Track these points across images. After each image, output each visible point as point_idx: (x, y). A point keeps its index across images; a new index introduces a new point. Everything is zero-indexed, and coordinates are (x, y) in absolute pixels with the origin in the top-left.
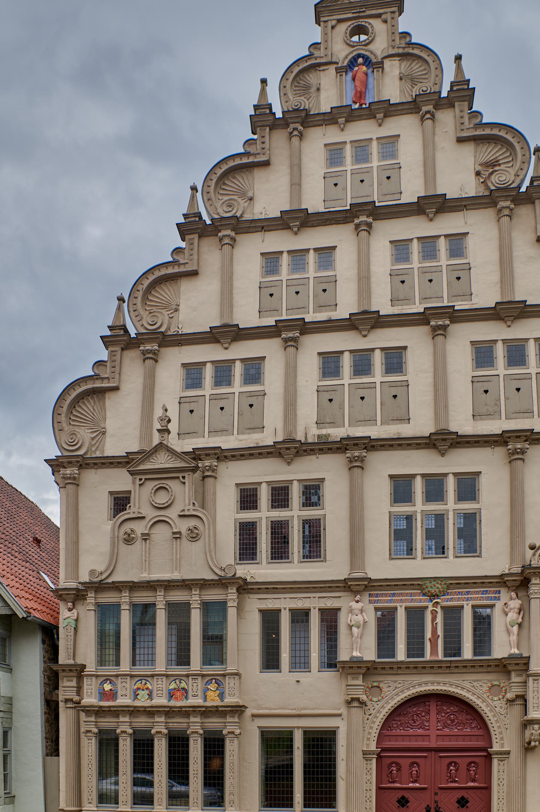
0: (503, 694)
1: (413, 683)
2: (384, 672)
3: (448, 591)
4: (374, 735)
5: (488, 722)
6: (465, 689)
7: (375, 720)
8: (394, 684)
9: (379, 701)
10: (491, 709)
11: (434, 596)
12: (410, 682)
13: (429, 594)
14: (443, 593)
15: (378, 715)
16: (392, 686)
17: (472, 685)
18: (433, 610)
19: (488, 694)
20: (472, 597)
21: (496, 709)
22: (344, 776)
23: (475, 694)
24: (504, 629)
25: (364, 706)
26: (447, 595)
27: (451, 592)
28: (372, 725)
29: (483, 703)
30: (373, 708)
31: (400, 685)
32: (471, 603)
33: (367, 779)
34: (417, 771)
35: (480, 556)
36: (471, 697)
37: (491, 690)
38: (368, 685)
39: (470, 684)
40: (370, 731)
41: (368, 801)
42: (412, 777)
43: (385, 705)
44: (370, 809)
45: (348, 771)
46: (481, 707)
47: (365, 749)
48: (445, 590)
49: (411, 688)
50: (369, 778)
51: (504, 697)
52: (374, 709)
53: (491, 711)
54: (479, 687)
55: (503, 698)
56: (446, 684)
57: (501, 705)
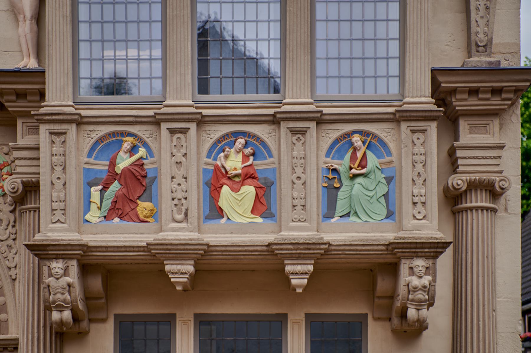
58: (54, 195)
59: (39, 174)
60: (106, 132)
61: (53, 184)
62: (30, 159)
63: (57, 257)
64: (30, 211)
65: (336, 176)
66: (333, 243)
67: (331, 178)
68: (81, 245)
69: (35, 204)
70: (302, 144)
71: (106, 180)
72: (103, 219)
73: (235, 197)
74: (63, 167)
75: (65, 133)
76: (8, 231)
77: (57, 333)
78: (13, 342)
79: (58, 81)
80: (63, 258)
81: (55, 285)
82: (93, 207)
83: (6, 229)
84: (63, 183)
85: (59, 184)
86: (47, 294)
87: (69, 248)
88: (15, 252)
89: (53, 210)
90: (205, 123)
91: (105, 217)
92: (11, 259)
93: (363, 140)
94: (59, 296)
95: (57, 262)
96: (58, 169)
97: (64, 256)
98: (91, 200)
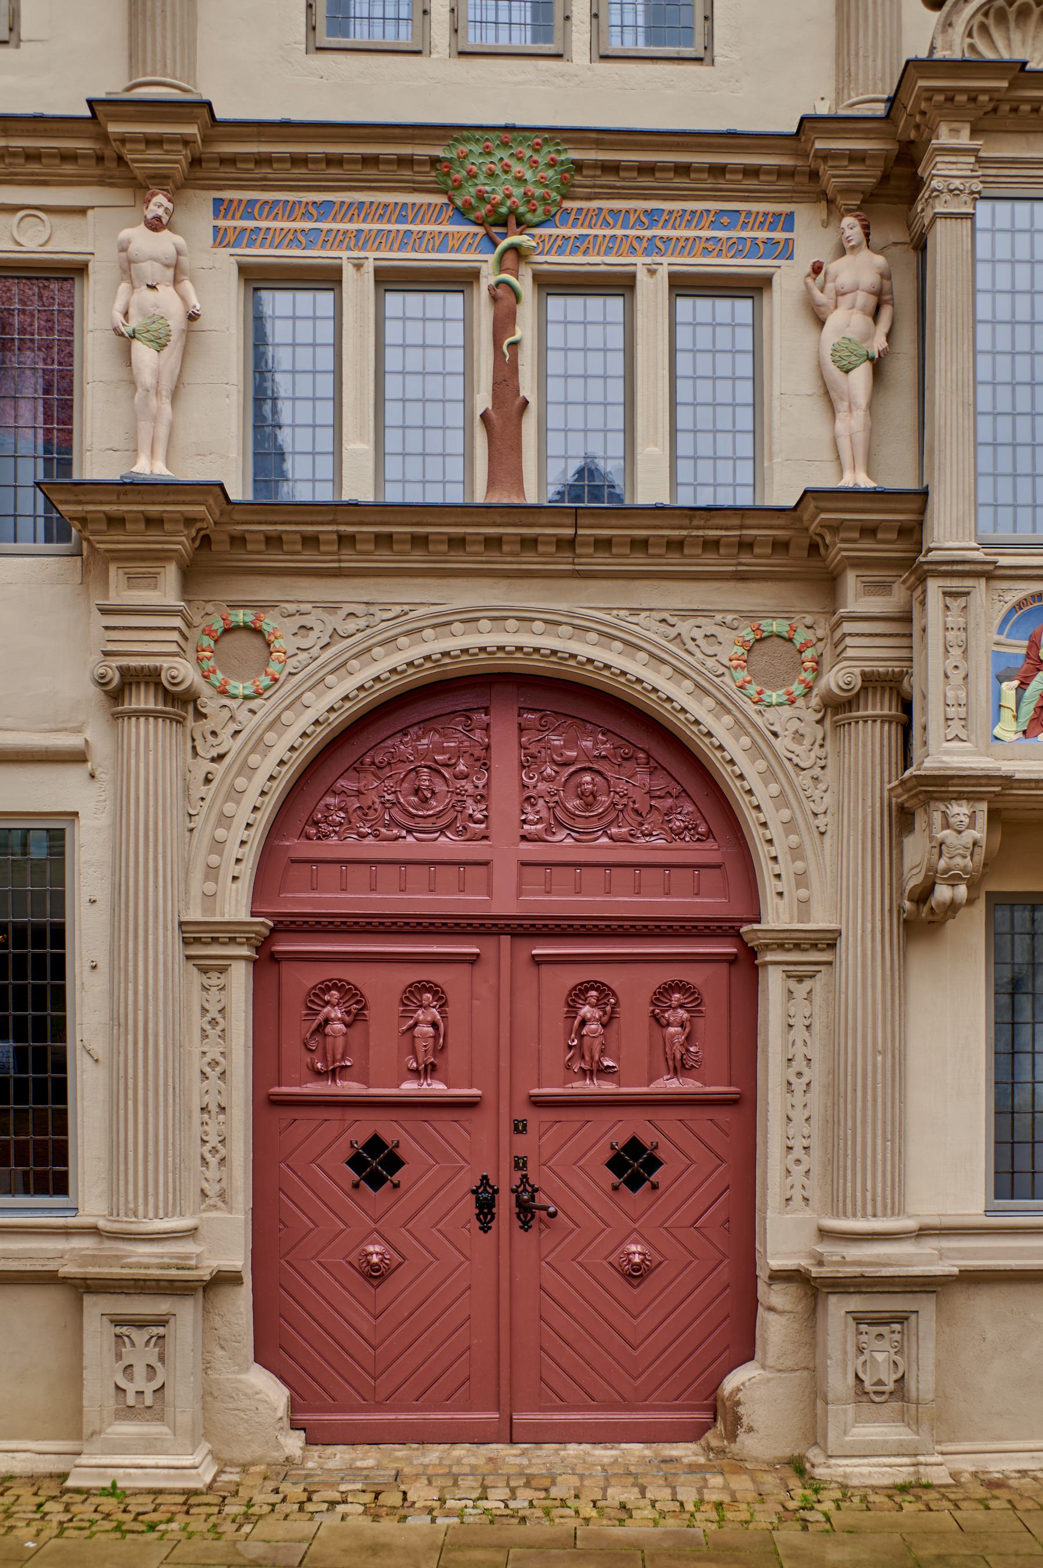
0: (808, 676)
1: (412, 615)
2: (277, 560)
3: (566, 204)
4: (238, 852)
5: (743, 802)
6: (640, 648)
7: (241, 783)
8: (325, 616)
9: (258, 694)
10: (754, 742)
11: (505, 224)
12: (397, 610)
13: (483, 211)
14: (546, 212)
15: (254, 760)
16: (318, 626)
17: (673, 632)
18: (499, 284)
19: (742, 675)
20: (670, 239)
21: (776, 743)
22: (99, 1045)
23: (686, 676)
24: (808, 384)
25: (190, 717)
26: (564, 224)
27: (580, 210)
28: (229, 808)
29: (718, 717)
30: (234, 727)
31: (351, 626)
32: (666, 264)
33: (207, 1059)
34: (434, 1025)
35: (708, 60)
36: (668, 688)
37: (755, 657)
38: (208, 620)
39: (664, 628)
40: (221, 833)
41: (213, 1161)
42: (414, 1052)
43: (287, 717)
44: (222, 1195)
45: (117, 1021)
46: (709, 734)
47: (195, 914)
48: (554, 195)
49: (403, 641)
50: (214, 1053)
51: (810, 689)
52: (237, 732)
53: (755, 751)
54: (701, 641)
55: (805, 695)
56: (559, 624)
57: (795, 724)
58: (948, 694)
59: (911, 659)
60: (1029, 592)
61: (946, 676)
62: (871, 635)
63: (959, 797)
64: (857, 722)
68: (1001, 777)
69: (874, 708)
71: (1025, 672)
72: (1020, 735)
74: (962, 649)
75: (968, 593)
76: (813, 754)
77: (905, 921)
78: (830, 935)
79: (954, 508)
80: (968, 799)
81: (956, 842)
82: (1007, 715)
83: (810, 750)
84: (963, 675)
85: (956, 677)
86: (936, 857)
87: (984, 782)
88: (824, 788)
89: (947, 719)
91: (1024, 732)
92: (818, 800)
94: (958, 860)
95: (958, 805)
96: (956, 652)
97: (970, 795)
98: (1002, 703)
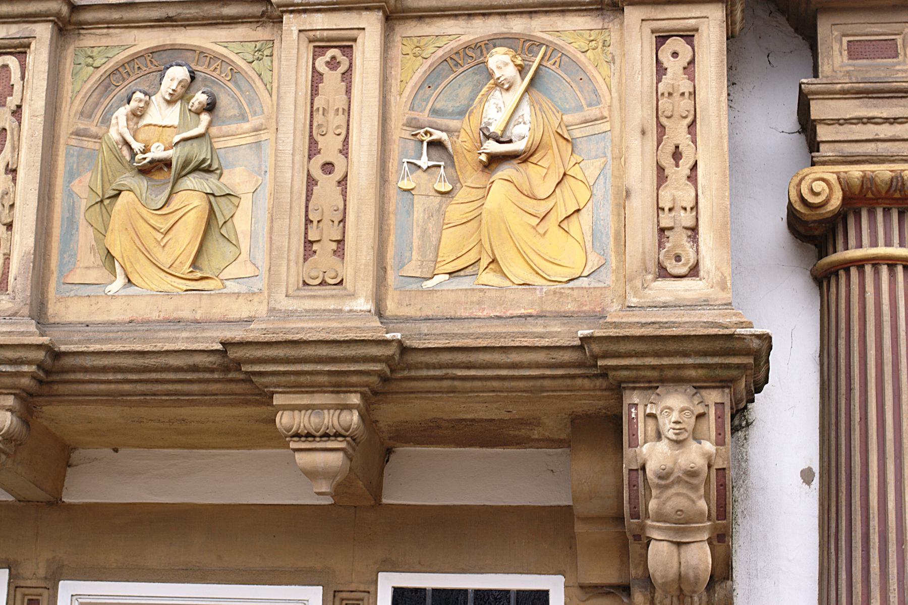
65: (442, 163)
66: (415, 344)
67: (425, 167)
70: (343, 74)
73: (152, 222)
90: (83, 29)
93: (519, 62)
